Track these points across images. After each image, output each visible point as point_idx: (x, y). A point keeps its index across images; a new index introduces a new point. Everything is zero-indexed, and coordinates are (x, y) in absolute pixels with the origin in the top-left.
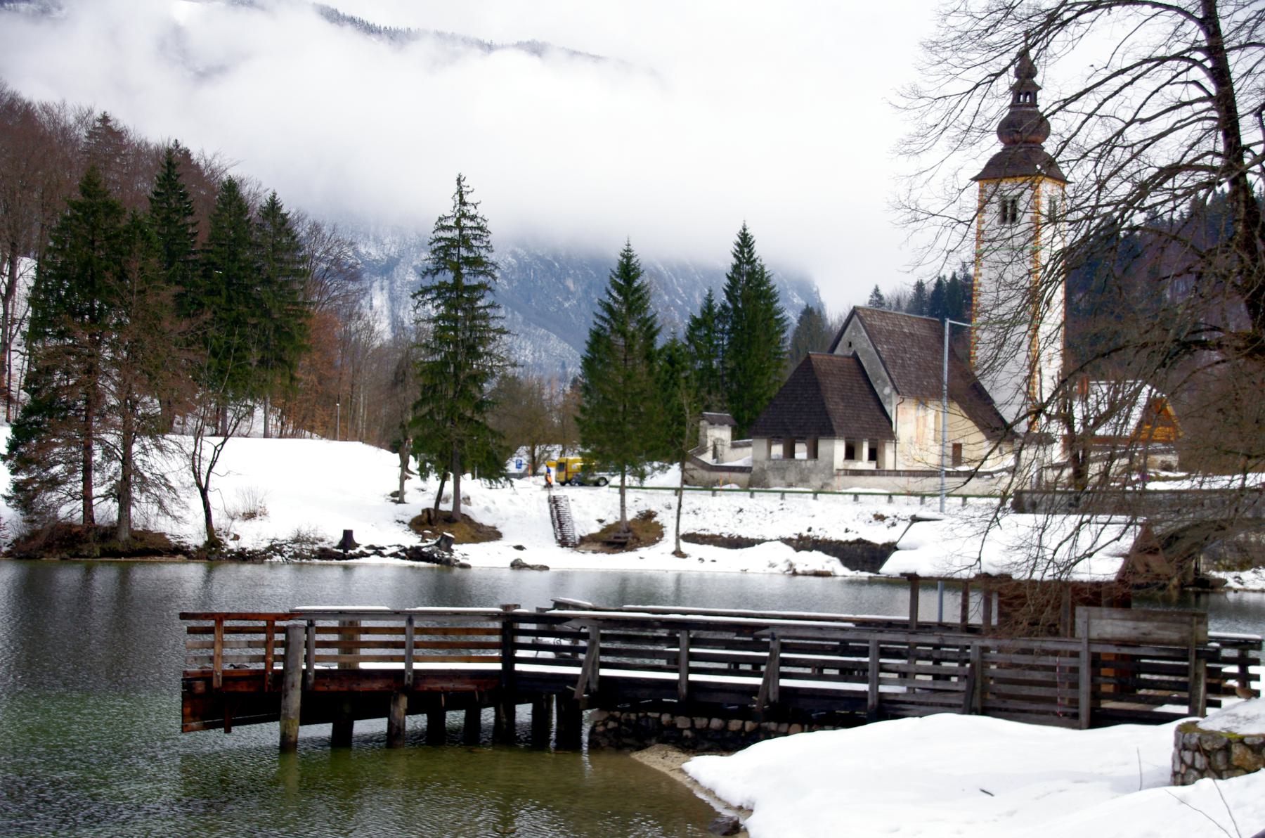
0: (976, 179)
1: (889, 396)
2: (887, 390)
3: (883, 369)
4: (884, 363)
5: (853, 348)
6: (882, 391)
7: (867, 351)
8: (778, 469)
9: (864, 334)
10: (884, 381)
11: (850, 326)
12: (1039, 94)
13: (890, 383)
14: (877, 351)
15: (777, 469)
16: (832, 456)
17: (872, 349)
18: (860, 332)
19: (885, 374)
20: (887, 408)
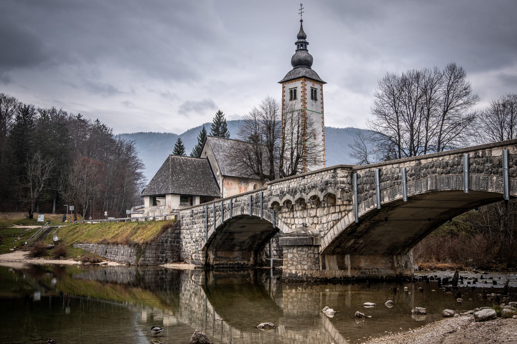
0: (280, 83)
1: (218, 176)
2: (218, 173)
3: (216, 163)
4: (217, 160)
5: (207, 155)
6: (216, 174)
7: (211, 156)
8: (153, 211)
9: (210, 148)
10: (217, 170)
11: (206, 145)
12: (307, 46)
13: (219, 170)
14: (215, 155)
15: (153, 211)
16: (171, 203)
17: (213, 155)
18: (209, 147)
19: (217, 166)
20: (218, 182)
